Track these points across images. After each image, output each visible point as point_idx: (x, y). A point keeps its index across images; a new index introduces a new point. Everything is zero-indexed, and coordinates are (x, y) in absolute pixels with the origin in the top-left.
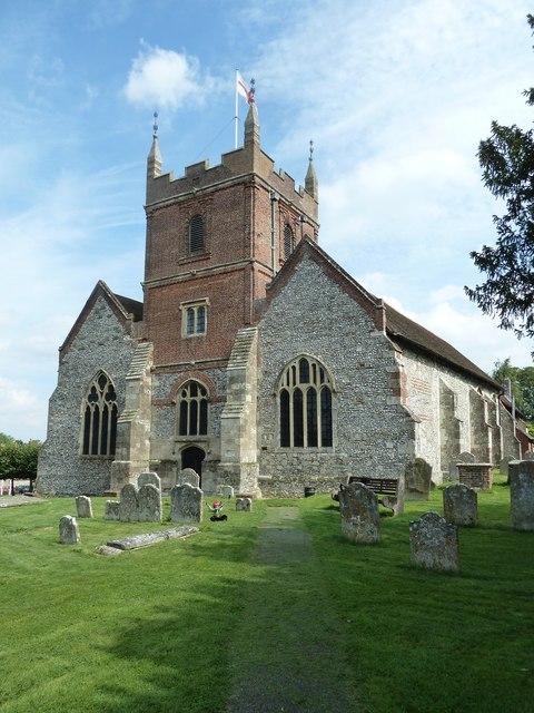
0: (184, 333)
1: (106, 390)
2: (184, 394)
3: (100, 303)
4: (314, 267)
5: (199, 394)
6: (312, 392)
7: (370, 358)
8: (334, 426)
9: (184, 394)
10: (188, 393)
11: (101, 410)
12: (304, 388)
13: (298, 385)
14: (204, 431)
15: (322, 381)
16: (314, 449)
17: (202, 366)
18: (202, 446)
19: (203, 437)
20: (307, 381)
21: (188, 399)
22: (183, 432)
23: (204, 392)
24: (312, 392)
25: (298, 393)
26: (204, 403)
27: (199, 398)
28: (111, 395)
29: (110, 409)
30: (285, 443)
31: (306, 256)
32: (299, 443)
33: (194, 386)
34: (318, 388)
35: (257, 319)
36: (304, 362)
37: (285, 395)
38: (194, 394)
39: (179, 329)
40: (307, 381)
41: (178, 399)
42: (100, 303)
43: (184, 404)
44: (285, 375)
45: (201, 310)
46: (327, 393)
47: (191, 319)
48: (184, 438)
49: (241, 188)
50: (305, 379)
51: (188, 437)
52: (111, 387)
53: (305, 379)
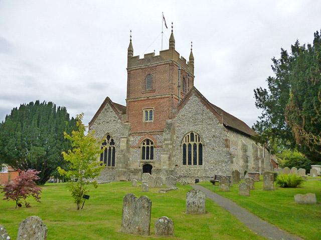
0: (144, 120)
1: (110, 141)
2: (144, 144)
3: (107, 106)
4: (197, 98)
5: (150, 143)
6: (195, 145)
7: (217, 134)
8: (203, 158)
9: (144, 144)
10: (146, 143)
11: (108, 149)
12: (192, 143)
13: (190, 142)
14: (152, 158)
15: (199, 141)
16: (196, 166)
17: (152, 133)
18: (151, 164)
19: (152, 161)
20: (194, 141)
21: (146, 146)
22: (143, 158)
23: (152, 143)
24: (195, 145)
25: (190, 145)
26: (152, 147)
27: (150, 145)
28: (112, 143)
29: (112, 148)
30: (184, 163)
31: (193, 94)
32: (190, 163)
33: (148, 141)
34: (197, 143)
35: (174, 117)
36: (192, 134)
37: (185, 145)
38: (148, 144)
39: (142, 119)
40: (194, 141)
41: (142, 145)
42: (107, 106)
43: (144, 147)
44: (185, 138)
45: (151, 111)
46: (201, 146)
47: (147, 115)
48: (144, 161)
49: (168, 65)
50: (192, 140)
51: (146, 160)
52: (112, 140)
53: (192, 140)
